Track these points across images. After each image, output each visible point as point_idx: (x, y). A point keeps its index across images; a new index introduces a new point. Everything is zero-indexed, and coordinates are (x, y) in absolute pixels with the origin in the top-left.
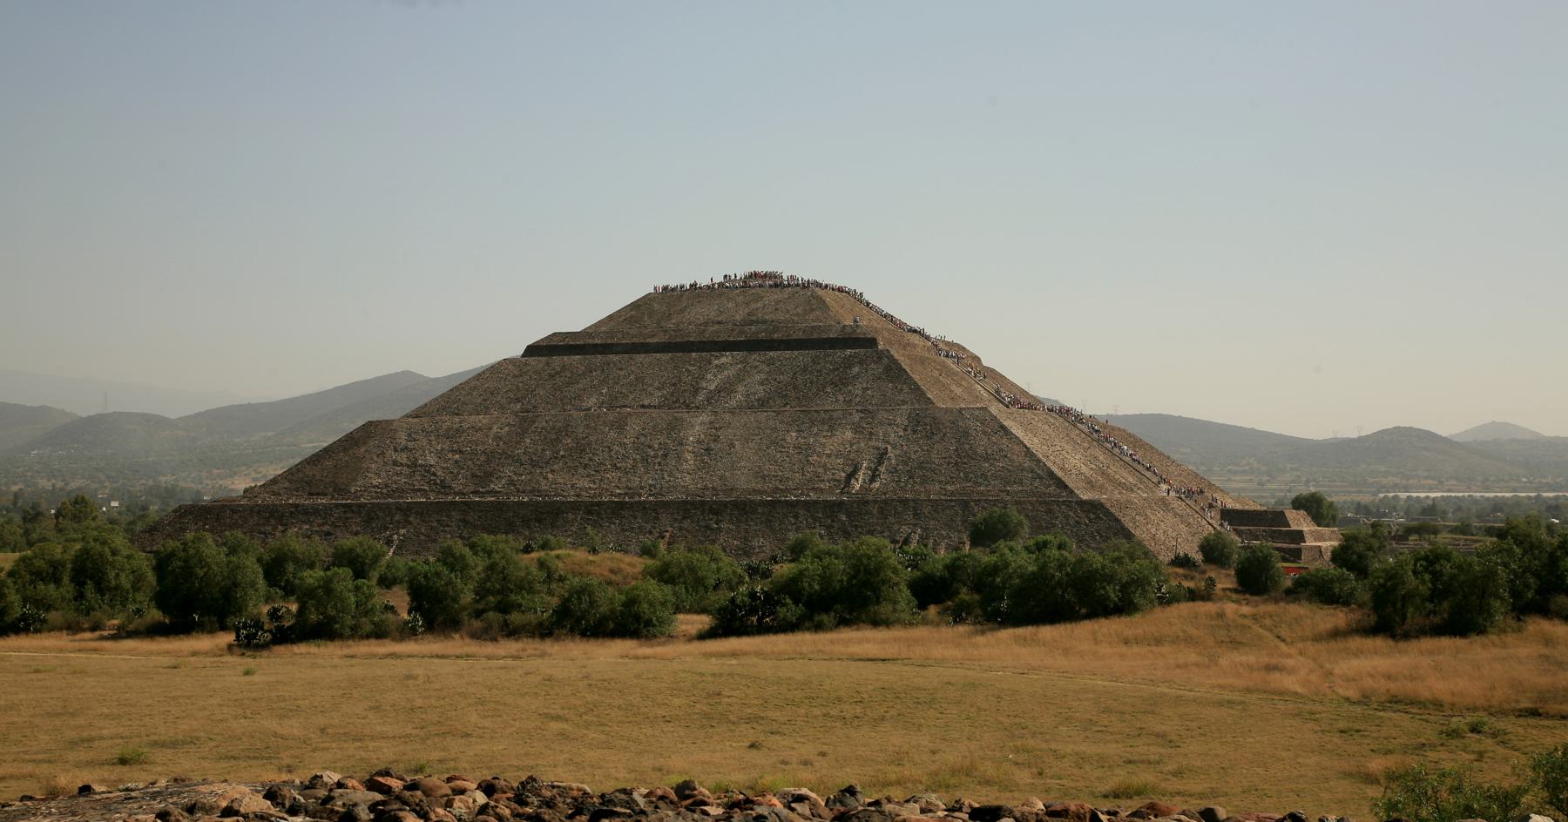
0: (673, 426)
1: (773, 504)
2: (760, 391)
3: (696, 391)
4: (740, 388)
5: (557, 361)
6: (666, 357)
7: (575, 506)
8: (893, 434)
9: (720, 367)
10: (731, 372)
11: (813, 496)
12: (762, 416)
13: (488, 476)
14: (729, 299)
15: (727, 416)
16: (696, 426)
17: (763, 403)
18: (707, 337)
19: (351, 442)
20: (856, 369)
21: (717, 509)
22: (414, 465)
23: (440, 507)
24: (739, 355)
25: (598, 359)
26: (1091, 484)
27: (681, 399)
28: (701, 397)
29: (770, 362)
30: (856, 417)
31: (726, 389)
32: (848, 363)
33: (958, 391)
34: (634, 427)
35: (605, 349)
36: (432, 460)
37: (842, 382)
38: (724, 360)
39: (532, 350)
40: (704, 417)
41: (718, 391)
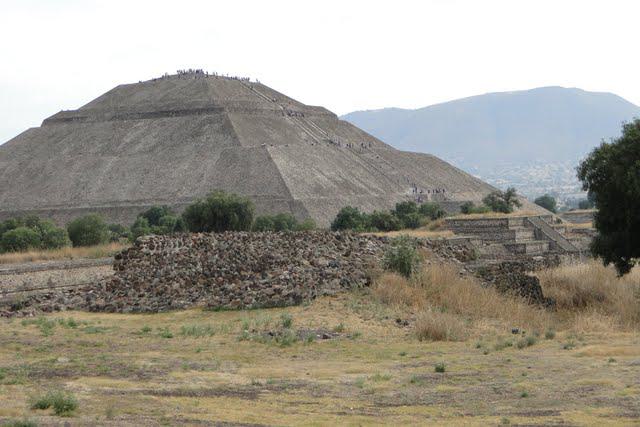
4: (143, 140)
8: (210, 164)
17: (151, 150)
32: (202, 124)
34: (77, 165)
39: (47, 122)
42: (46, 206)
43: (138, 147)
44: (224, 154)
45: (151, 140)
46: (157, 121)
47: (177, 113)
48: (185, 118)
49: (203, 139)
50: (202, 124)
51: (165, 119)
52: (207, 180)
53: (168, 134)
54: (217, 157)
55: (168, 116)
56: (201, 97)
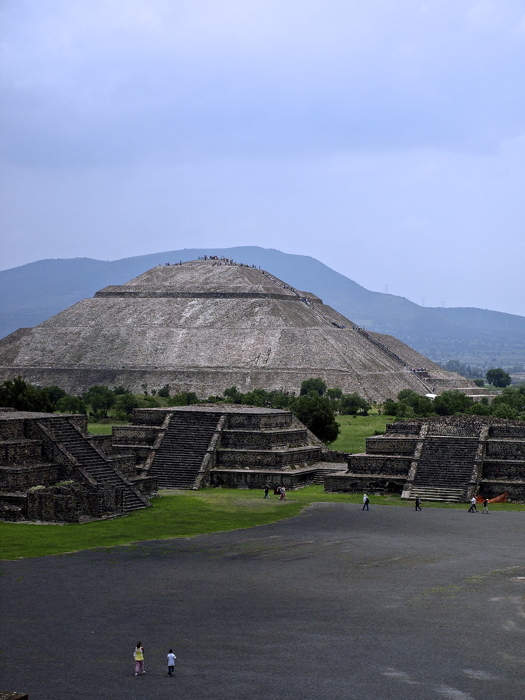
0: (168, 335)
1: (216, 373)
2: (211, 319)
3: (180, 318)
5: (112, 300)
6: (164, 300)
7: (122, 372)
8: (274, 340)
9: (192, 306)
10: (198, 308)
11: (236, 370)
12: (211, 330)
13: (79, 358)
14: (197, 271)
15: (195, 331)
16: (181, 334)
17: (212, 325)
18: (185, 290)
19: (12, 339)
20: (257, 309)
21: (189, 375)
22: (44, 350)
23: (59, 371)
24: (201, 300)
25: (132, 300)
26: (365, 367)
27: (171, 322)
28: (182, 321)
29: (216, 304)
30: (256, 333)
31: (194, 317)
33: (307, 319)
34: (151, 334)
35: (135, 295)
36: (51, 347)
37: (250, 314)
38: (193, 302)
39: (99, 294)
40: (184, 331)
41: (191, 317)
42: (132, 367)
43: (199, 322)
44: (283, 332)
45: (208, 316)
46: (209, 301)
47: (225, 295)
48: (237, 300)
49: (258, 318)
50: (253, 306)
51: (217, 300)
52: (276, 355)
53: (223, 312)
54: (278, 335)
55: (216, 297)
56: (240, 283)
